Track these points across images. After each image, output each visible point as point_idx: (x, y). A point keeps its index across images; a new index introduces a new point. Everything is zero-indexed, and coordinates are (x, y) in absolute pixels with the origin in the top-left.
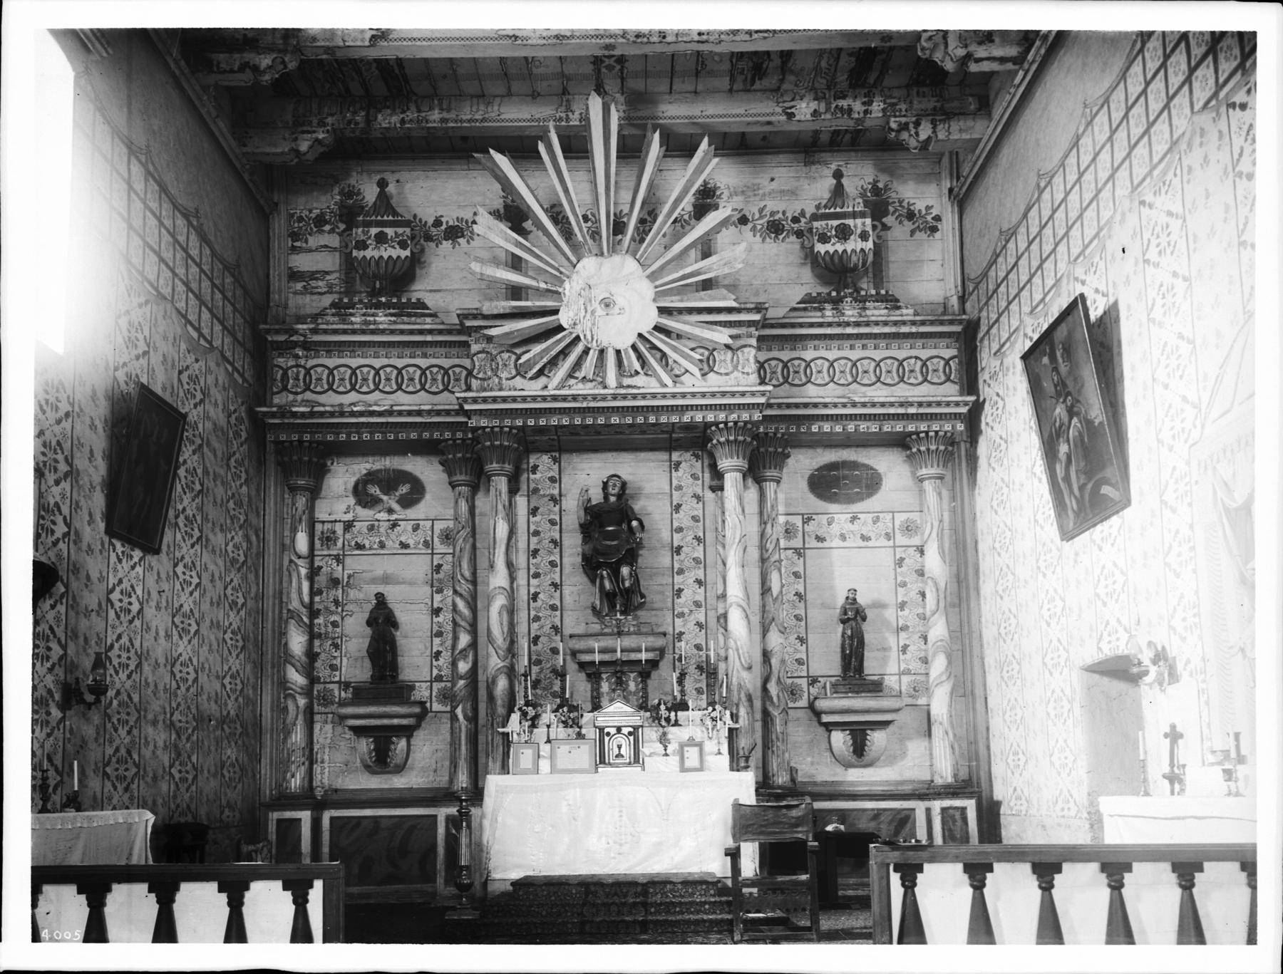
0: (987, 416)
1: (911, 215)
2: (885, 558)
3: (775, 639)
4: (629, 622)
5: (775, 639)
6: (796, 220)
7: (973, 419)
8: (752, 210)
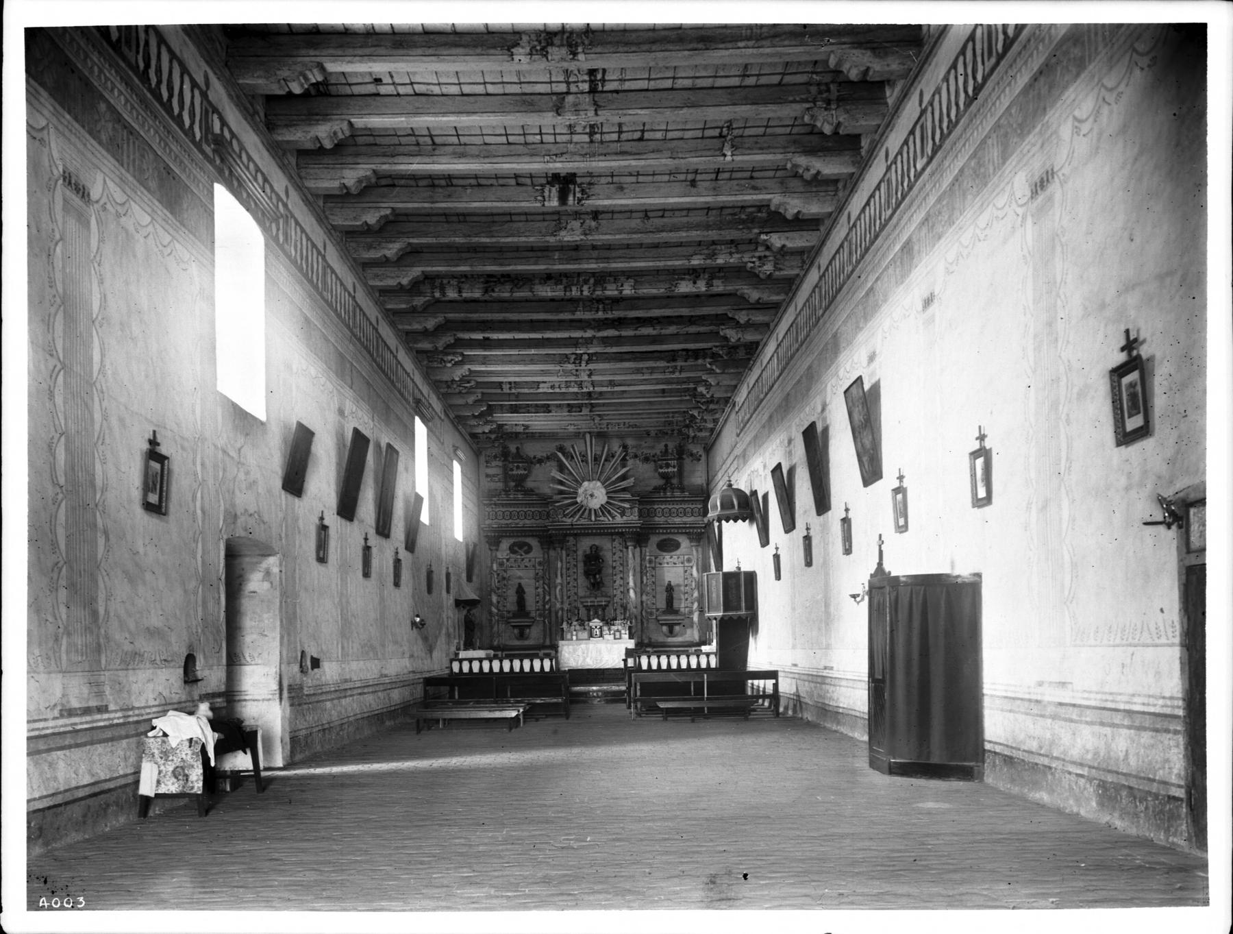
1: (692, 455)
2: (681, 570)
3: (644, 598)
4: (598, 593)
5: (644, 598)
8: (639, 453)
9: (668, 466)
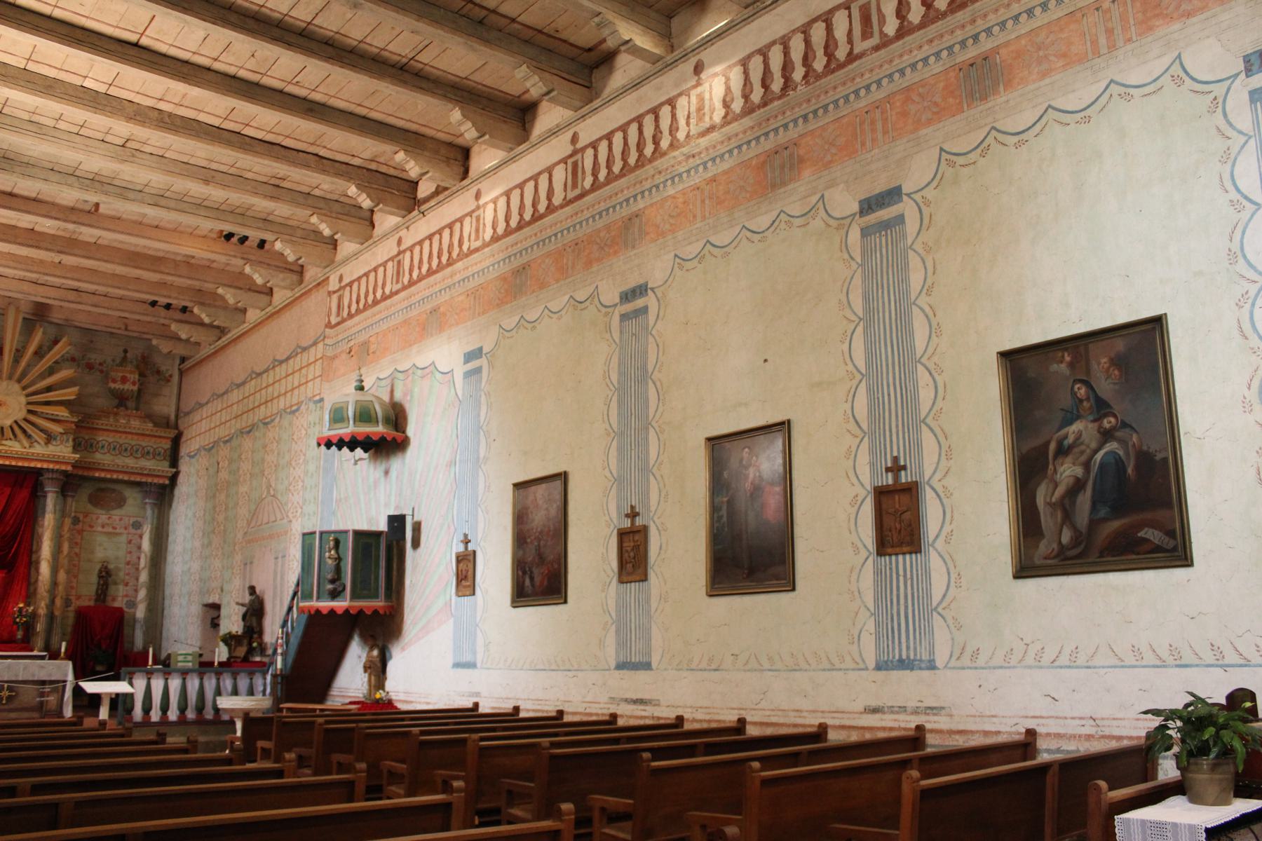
0: (181, 479)
1: (158, 372)
6: (101, 364)
7: (174, 479)
9: (124, 380)
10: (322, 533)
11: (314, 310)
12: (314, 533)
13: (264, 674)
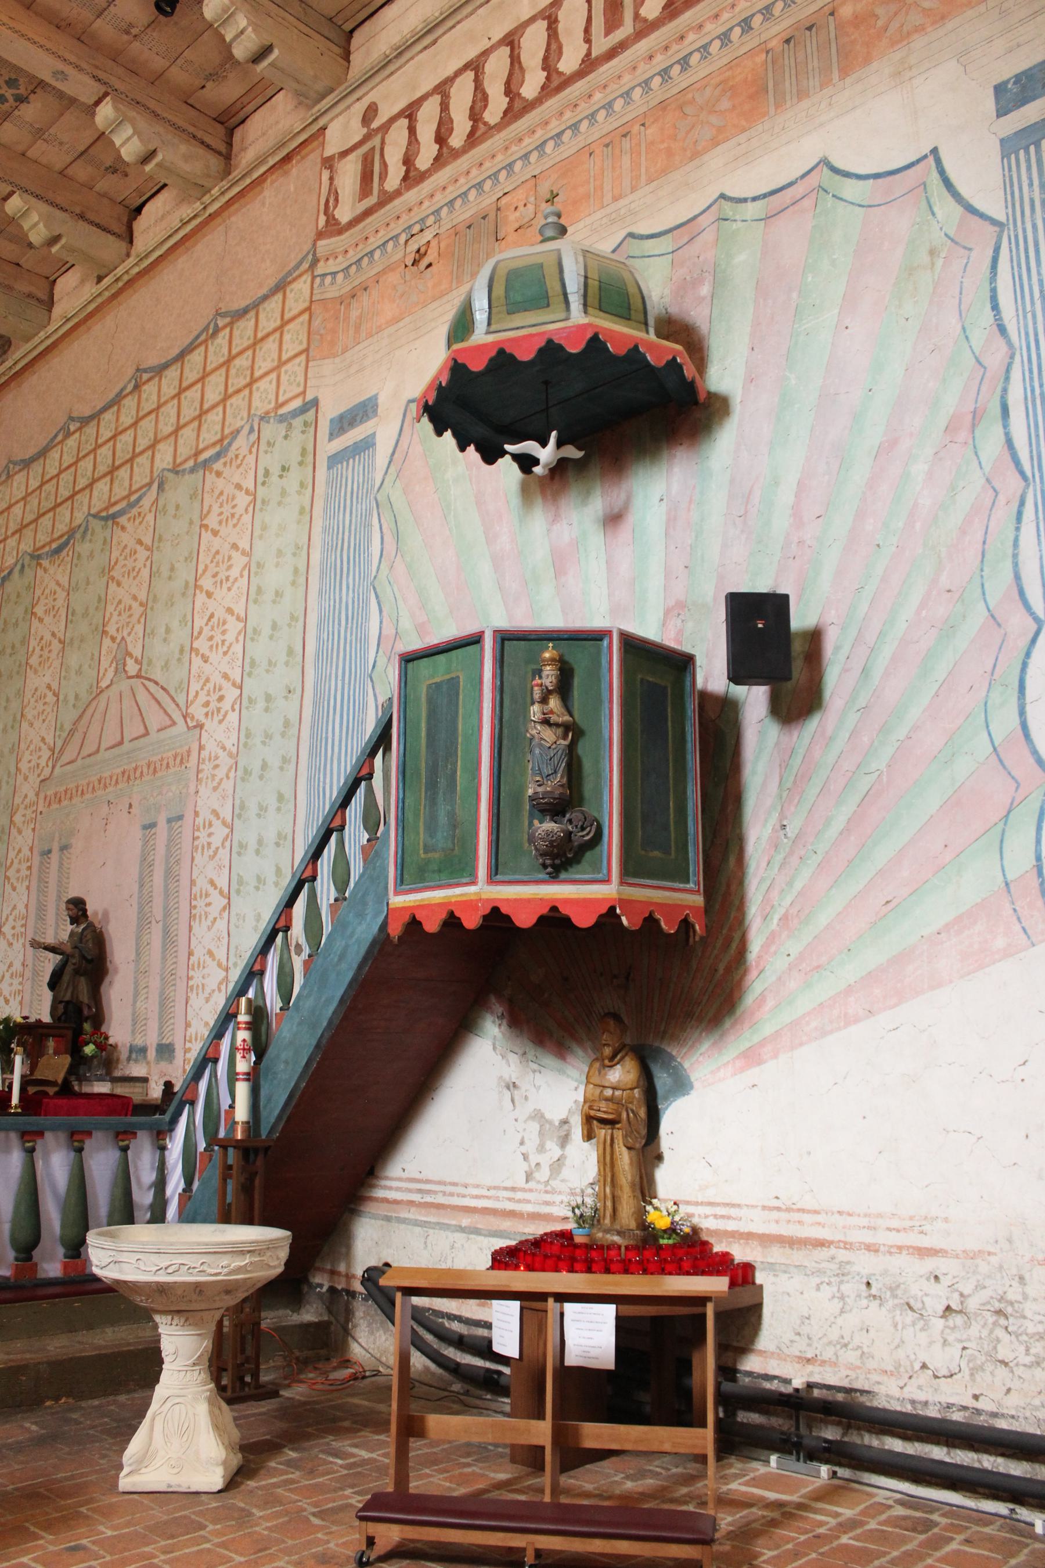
10: (505, 638)
11: (274, 222)
12: (476, 640)
13: (161, 1135)
